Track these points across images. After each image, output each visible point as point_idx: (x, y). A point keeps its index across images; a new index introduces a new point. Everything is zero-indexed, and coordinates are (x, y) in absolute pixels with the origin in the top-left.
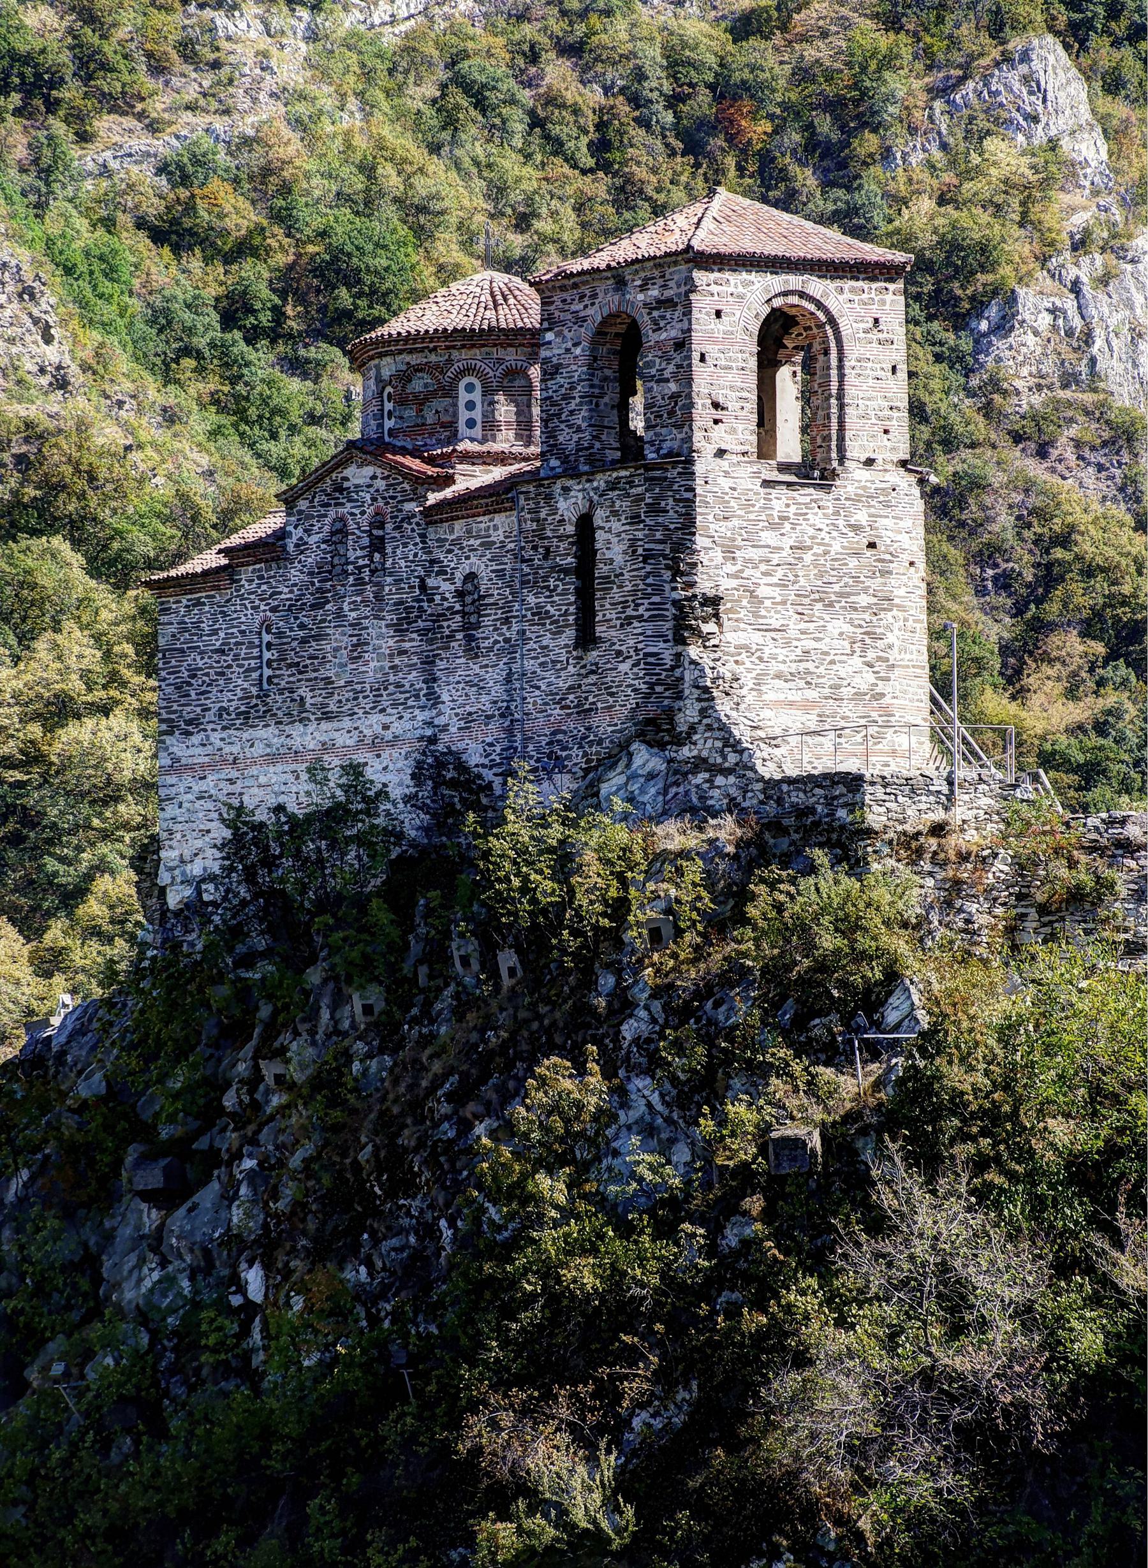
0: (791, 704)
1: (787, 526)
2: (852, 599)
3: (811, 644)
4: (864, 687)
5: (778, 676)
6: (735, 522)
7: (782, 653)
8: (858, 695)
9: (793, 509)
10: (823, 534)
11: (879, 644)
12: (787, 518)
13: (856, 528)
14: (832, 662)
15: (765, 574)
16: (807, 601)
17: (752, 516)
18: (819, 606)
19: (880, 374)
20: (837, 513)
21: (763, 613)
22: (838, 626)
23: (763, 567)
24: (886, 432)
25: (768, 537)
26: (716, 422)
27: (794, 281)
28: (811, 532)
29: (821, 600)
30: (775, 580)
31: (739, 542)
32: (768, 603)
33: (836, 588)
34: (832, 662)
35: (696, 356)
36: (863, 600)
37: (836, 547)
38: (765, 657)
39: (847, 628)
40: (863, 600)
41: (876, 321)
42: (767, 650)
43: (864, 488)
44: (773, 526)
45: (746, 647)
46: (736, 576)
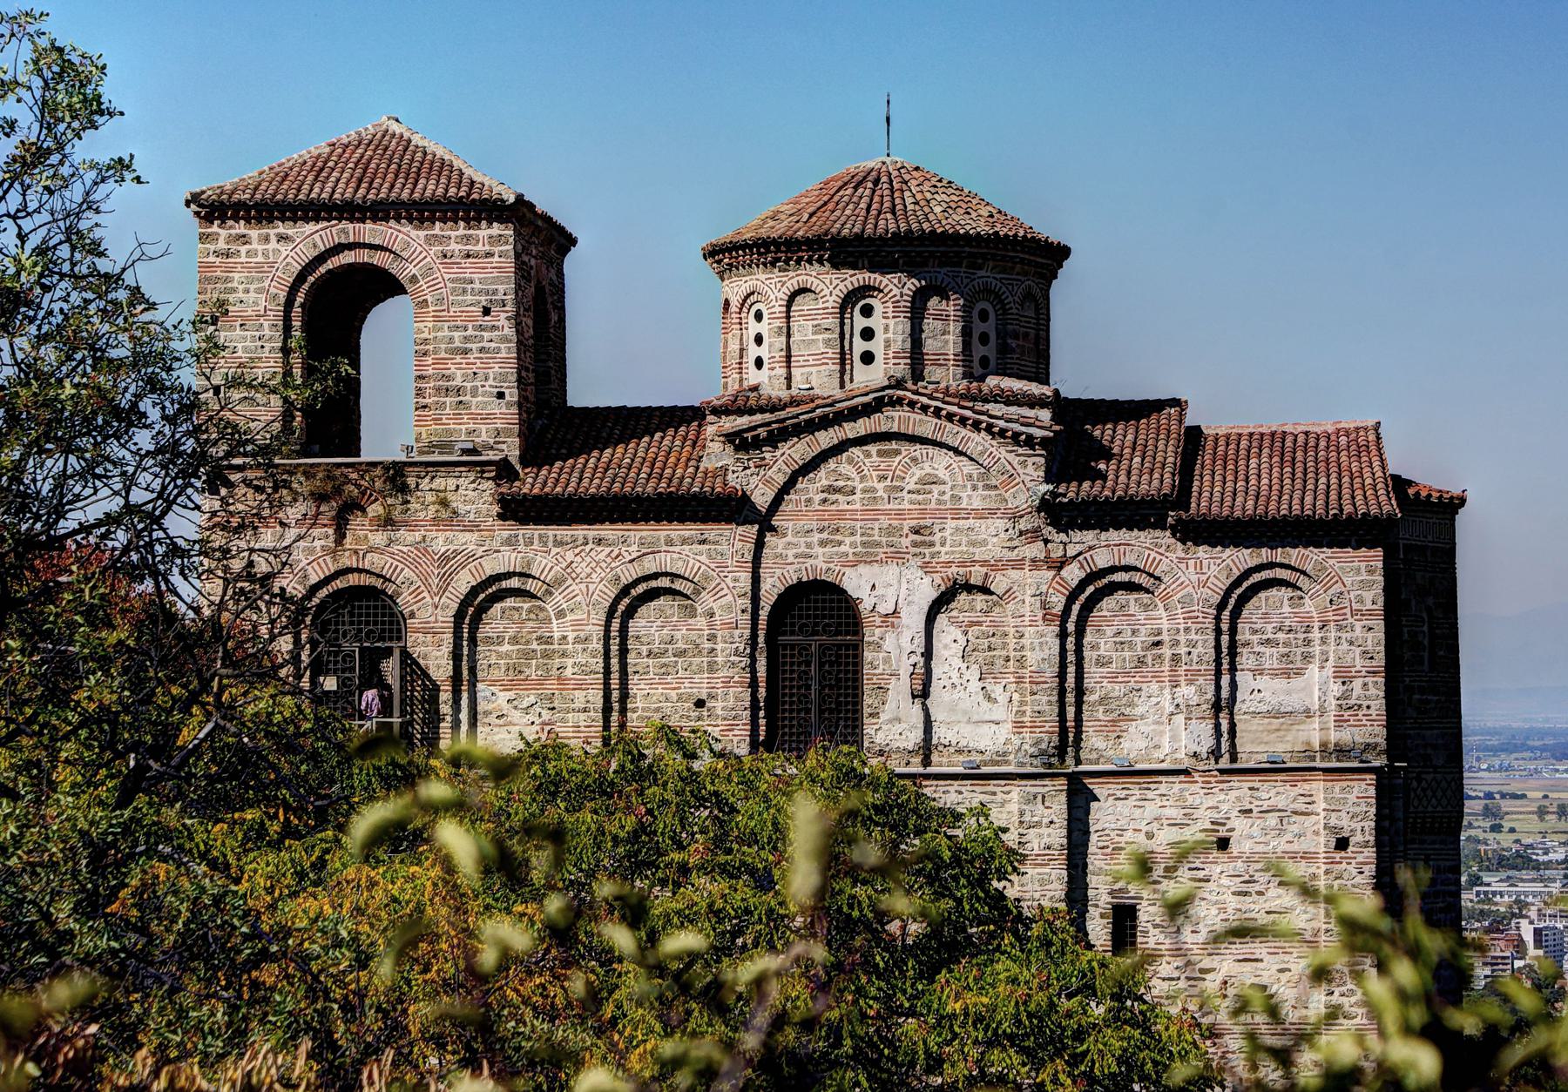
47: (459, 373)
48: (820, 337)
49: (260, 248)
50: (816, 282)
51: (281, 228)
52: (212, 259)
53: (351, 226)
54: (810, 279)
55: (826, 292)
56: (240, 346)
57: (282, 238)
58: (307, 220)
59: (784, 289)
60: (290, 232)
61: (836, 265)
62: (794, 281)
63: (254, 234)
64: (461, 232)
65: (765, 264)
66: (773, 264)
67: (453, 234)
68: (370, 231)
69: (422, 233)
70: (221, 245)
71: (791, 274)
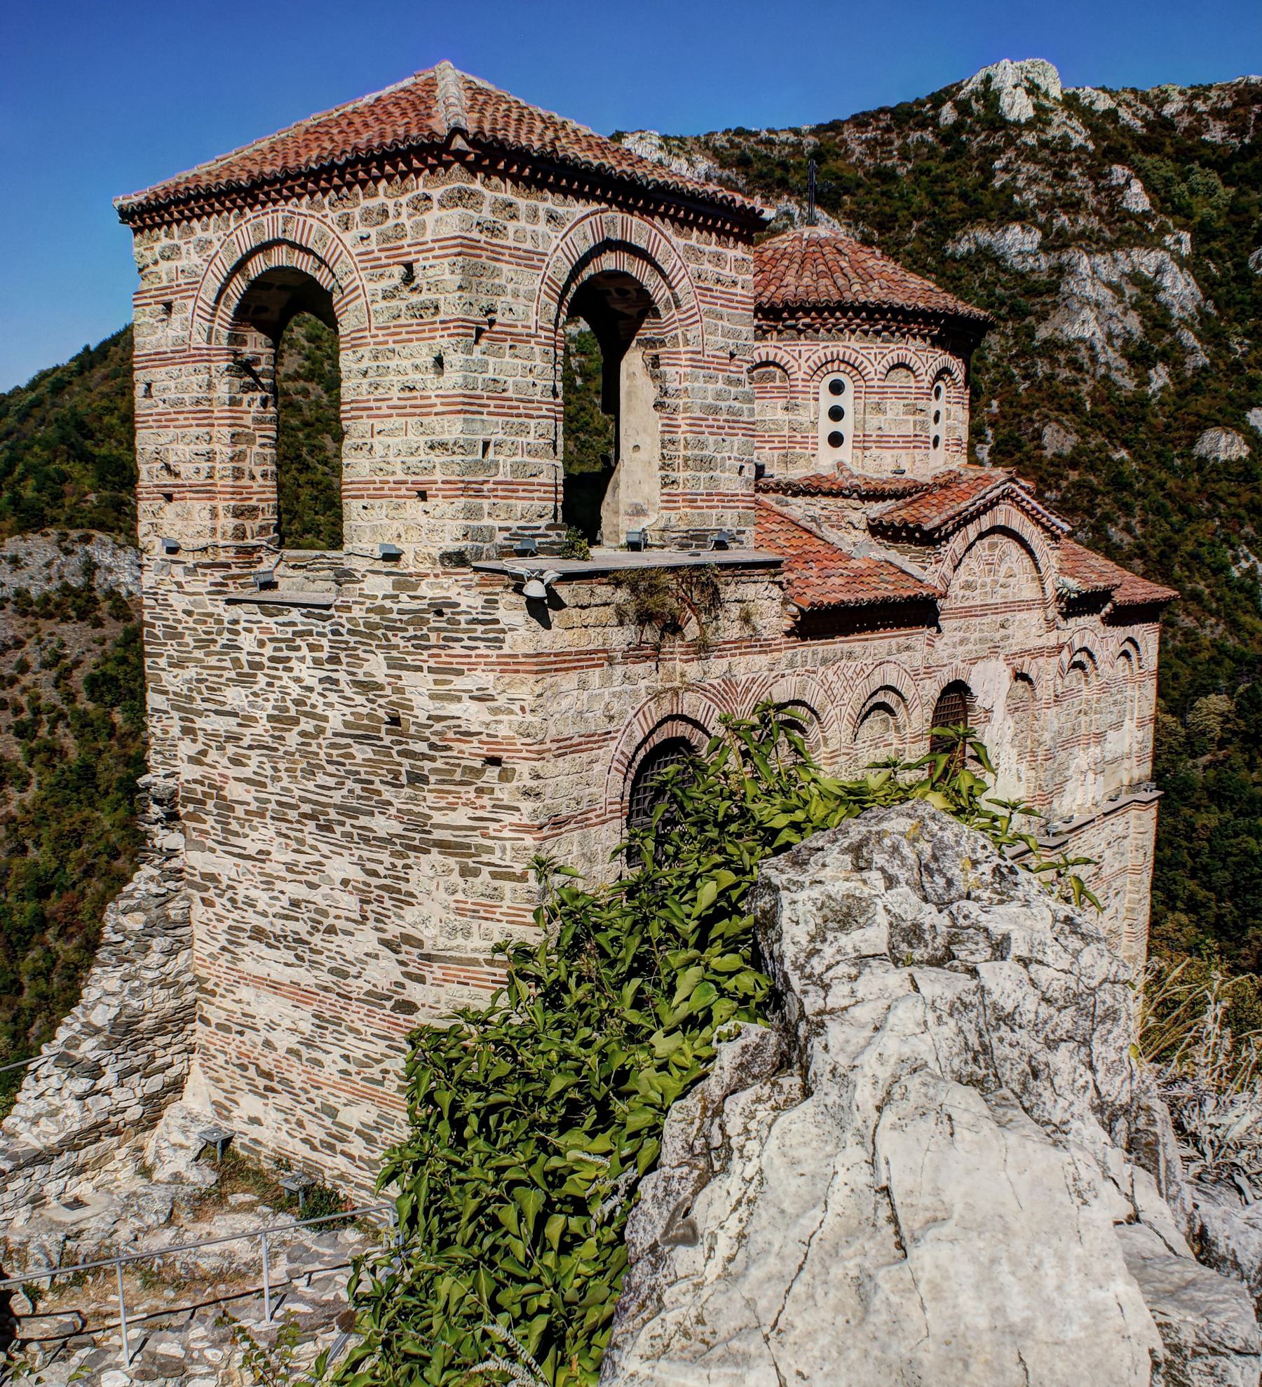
0: (275, 986)
1: (262, 680)
2: (363, 821)
3: (302, 892)
4: (384, 985)
5: (258, 934)
6: (191, 672)
7: (262, 898)
8: (375, 998)
9: (268, 651)
10: (314, 698)
11: (408, 912)
12: (259, 666)
13: (367, 686)
14: (331, 930)
15: (236, 761)
16: (293, 815)
17: (213, 661)
18: (311, 826)
19: (415, 377)
20: (334, 659)
21: (234, 826)
22: (341, 867)
23: (231, 749)
24: (423, 496)
25: (235, 697)
26: (169, 498)
27: (267, 221)
28: (295, 691)
29: (312, 817)
30: (247, 772)
31: (199, 705)
32: (240, 811)
33: (337, 797)
34: (331, 930)
35: (139, 390)
36: (382, 825)
37: (335, 721)
38: (240, 898)
39: (356, 874)
40: (382, 825)
41: (409, 266)
42: (241, 892)
43: (381, 610)
44: (244, 680)
45: (213, 878)
46: (195, 760)
47: (712, 439)
48: (911, 418)
49: (529, 227)
50: (915, 358)
51: (550, 202)
52: (475, 234)
53: (620, 215)
54: (910, 355)
55: (922, 370)
56: (510, 380)
57: (552, 218)
58: (579, 195)
59: (884, 362)
60: (561, 210)
61: (936, 342)
62: (894, 354)
63: (522, 203)
64: (713, 248)
65: (866, 333)
66: (878, 333)
67: (707, 248)
68: (639, 229)
69: (679, 242)
70: (486, 214)
71: (892, 346)
